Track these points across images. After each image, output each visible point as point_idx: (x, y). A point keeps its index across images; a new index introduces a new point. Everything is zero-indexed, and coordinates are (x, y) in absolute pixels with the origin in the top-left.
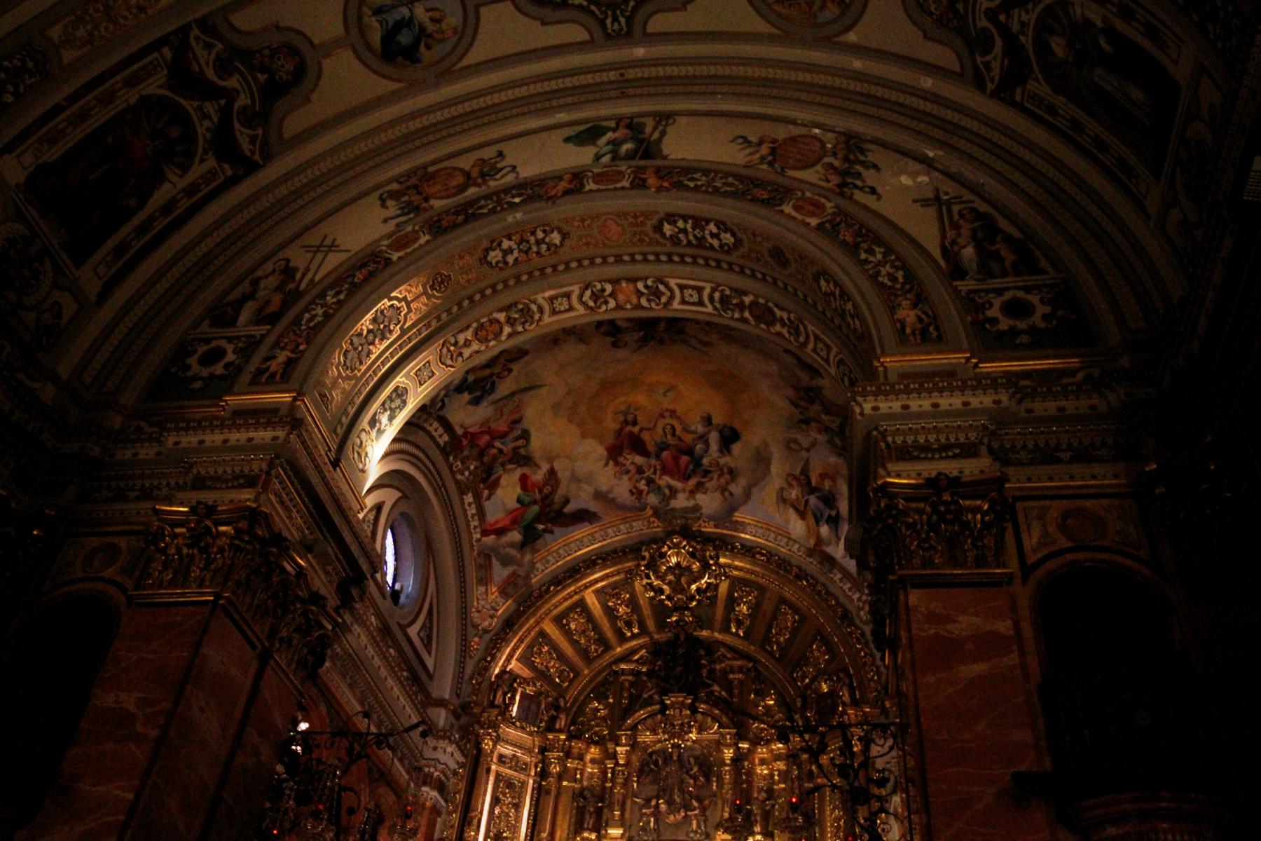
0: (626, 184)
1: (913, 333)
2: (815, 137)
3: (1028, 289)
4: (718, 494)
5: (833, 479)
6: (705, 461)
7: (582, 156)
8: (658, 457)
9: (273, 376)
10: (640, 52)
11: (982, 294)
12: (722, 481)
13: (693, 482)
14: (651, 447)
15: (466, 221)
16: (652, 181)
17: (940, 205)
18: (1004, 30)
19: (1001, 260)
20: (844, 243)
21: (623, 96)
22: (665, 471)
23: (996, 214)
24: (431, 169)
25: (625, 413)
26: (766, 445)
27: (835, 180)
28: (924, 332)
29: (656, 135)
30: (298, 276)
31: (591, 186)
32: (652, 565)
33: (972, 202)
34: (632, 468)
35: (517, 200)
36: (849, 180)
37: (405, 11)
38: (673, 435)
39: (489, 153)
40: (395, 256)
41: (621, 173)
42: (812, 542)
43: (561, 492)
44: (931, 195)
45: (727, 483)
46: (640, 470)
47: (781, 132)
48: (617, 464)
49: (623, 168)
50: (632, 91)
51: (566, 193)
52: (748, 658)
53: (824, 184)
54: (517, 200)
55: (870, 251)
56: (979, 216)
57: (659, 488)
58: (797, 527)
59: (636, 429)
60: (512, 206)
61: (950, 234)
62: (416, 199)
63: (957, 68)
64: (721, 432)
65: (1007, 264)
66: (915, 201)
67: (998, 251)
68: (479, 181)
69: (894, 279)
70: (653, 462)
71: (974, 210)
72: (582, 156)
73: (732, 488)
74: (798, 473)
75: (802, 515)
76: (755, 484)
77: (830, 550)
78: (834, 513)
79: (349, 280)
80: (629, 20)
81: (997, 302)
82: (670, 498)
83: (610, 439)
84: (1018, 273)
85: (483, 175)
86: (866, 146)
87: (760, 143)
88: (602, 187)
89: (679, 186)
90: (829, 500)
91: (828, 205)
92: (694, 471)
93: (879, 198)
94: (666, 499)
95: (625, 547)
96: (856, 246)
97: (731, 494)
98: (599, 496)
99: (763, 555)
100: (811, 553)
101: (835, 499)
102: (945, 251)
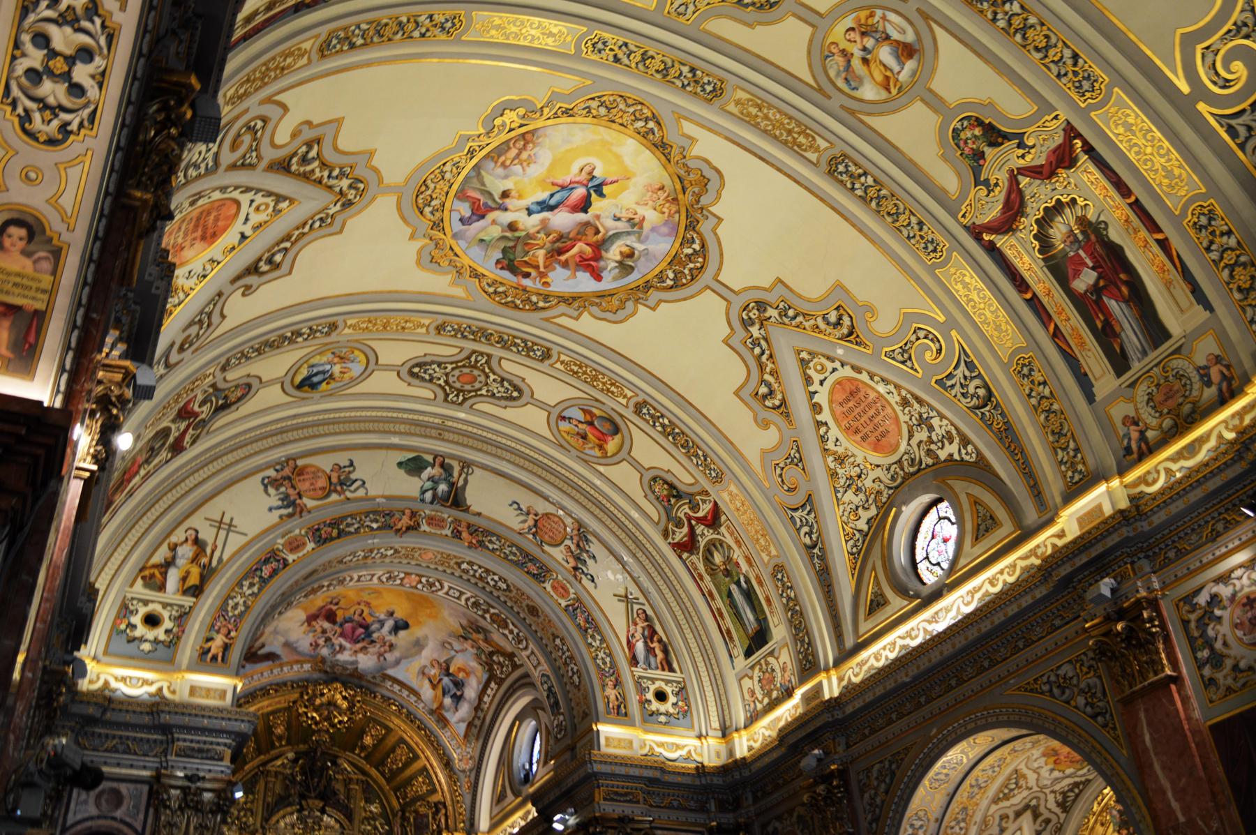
0: (448, 532)
2: (559, 517)
3: (667, 682)
4: (375, 657)
5: (468, 674)
6: (375, 635)
7: (410, 486)
8: (341, 625)
9: (214, 658)
10: (462, 415)
12: (382, 649)
13: (359, 645)
14: (339, 619)
15: (339, 536)
16: (465, 535)
17: (628, 602)
18: (692, 528)
19: (656, 656)
20: (579, 626)
21: (440, 438)
22: (342, 635)
23: (656, 621)
24: (300, 463)
25: (333, 598)
26: (426, 637)
27: (572, 563)
28: (619, 707)
29: (461, 483)
30: (209, 551)
31: (424, 527)
32: (311, 700)
33: (644, 604)
34: (319, 630)
35: (375, 526)
36: (580, 566)
37: (328, 367)
38: (361, 615)
39: (342, 458)
40: (291, 558)
41: (443, 520)
42: (435, 706)
43: (262, 640)
44: (623, 593)
45: (385, 652)
46: (324, 632)
47: (542, 507)
48: (309, 625)
49: (446, 516)
50: (447, 435)
51: (409, 528)
52: (364, 773)
53: (565, 564)
54: (375, 526)
55: (593, 637)
56: (647, 618)
57: (333, 645)
58: (427, 692)
59: (334, 608)
60: (372, 529)
61: (632, 628)
62: (291, 491)
63: (656, 519)
64: (396, 622)
65: (658, 661)
66: (615, 595)
67: (654, 649)
68: (339, 488)
69: (605, 663)
70: (337, 628)
71: (644, 611)
72: (410, 486)
73: (387, 656)
74: (441, 661)
75: (434, 687)
76: (406, 657)
77: (447, 715)
78: (459, 693)
79: (258, 573)
80: (465, 400)
81: (652, 688)
82: (338, 652)
83: (313, 610)
84: (663, 669)
85: (342, 484)
86: (590, 537)
87: (528, 513)
88: (433, 531)
89: (481, 543)
90: (459, 685)
91: (572, 591)
92: (363, 639)
93: (596, 587)
94: (334, 653)
95: (293, 682)
96: (586, 630)
97: (385, 659)
98: (287, 645)
100: (432, 712)
101: (463, 685)
102: (629, 642)
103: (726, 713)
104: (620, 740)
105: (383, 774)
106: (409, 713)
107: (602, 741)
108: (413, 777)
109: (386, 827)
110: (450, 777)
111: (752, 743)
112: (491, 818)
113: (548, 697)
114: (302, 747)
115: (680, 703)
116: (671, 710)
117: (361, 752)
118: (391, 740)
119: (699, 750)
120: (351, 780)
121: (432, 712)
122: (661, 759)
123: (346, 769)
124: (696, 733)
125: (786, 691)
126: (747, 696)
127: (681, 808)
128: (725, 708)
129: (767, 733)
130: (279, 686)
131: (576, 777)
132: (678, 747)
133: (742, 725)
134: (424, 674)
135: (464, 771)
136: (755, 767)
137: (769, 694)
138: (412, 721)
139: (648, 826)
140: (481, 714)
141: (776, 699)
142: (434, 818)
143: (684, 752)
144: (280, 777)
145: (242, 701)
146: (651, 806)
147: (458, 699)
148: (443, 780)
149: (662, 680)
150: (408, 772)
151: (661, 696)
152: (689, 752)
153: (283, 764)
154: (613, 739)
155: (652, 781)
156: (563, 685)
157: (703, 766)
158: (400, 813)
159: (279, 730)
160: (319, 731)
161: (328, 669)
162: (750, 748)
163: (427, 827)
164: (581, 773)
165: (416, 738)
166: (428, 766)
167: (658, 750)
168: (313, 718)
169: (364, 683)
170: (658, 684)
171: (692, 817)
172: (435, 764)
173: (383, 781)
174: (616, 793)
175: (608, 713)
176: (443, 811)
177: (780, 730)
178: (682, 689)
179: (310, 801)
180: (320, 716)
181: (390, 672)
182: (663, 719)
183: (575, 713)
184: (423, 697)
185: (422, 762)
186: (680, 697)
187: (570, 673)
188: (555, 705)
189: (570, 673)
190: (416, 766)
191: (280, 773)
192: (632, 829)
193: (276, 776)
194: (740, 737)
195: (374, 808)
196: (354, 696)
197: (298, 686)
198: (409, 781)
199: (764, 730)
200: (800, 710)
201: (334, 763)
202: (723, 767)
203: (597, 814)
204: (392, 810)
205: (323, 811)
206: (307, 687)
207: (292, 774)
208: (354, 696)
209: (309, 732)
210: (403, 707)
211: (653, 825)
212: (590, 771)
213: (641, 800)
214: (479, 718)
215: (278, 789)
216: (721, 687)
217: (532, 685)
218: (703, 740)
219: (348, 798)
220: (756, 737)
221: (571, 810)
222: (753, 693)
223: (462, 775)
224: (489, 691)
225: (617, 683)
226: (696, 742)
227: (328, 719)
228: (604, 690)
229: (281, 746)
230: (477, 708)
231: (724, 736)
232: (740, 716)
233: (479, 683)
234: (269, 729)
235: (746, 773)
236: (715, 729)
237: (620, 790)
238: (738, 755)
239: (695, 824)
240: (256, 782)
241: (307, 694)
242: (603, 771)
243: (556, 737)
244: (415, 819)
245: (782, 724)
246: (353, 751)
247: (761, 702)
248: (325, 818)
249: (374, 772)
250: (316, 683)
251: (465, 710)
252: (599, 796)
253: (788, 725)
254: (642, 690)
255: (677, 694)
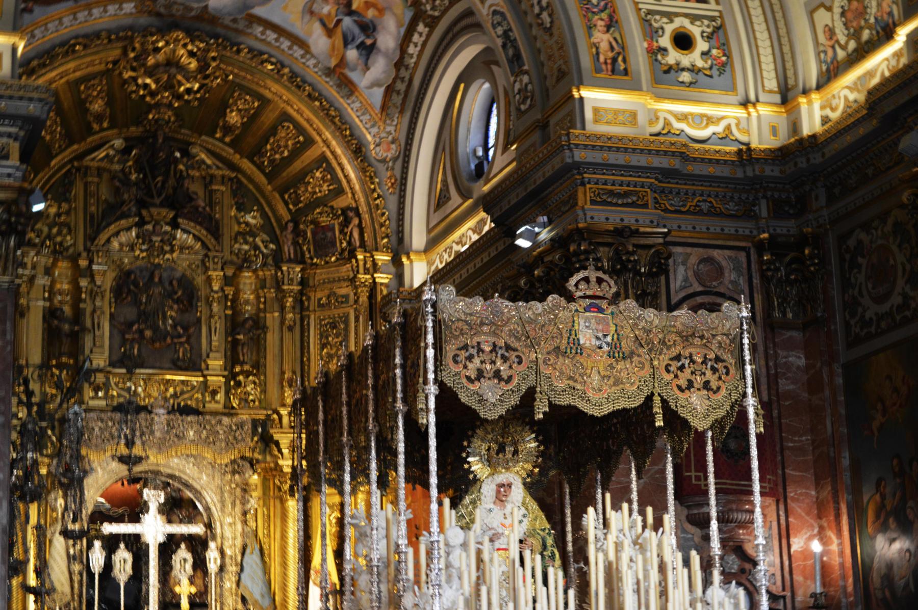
1: (606, 63)
3: (694, 18)
5: (381, 11)
11: (658, 17)
28: (614, 60)
32: (141, 58)
42: (333, 63)
52: (232, 167)
58: (319, 41)
75: (330, 32)
77: (354, 76)
78: (369, 42)
81: (669, 29)
90: (368, 28)
95: (109, 32)
99: (272, 64)
100: (329, 72)
101: (375, 29)
103: (789, 65)
104: (616, 112)
105: (260, 167)
106: (294, 75)
107: (589, 114)
108: (306, 172)
109: (272, 246)
110: (364, 171)
111: (828, 112)
112: (429, 231)
113: (504, 46)
114: (134, 130)
115: (714, 52)
116: (700, 63)
117: (224, 136)
118: (268, 118)
119: (744, 124)
120: (212, 177)
121: (329, 72)
122: (683, 139)
123: (203, 162)
124: (740, 97)
125: (884, 29)
126: (822, 38)
127: (713, 213)
128: (788, 57)
129: (852, 96)
130: (90, 39)
131: (548, 170)
132: (710, 120)
133: (813, 83)
134: (312, 13)
135: (383, 161)
136: (830, 151)
137: (855, 35)
138: (299, 87)
139: (661, 240)
140: (404, 73)
141: (867, 42)
142: (341, 232)
143: (719, 128)
144: (106, 176)
145: (35, 63)
146: (666, 210)
147: (368, 50)
148: (352, 175)
149: (686, 15)
150: (298, 165)
151: (683, 41)
152: (728, 127)
153: (107, 156)
154: (606, 110)
155: (667, 174)
156: (526, 28)
157: (749, 149)
158: (291, 225)
159: (97, 106)
160: (158, 105)
161: (162, 10)
162: (825, 120)
163: (333, 244)
164: (556, 163)
165: (308, 113)
166: (329, 154)
167: (678, 125)
168: (146, 86)
169: (219, 30)
170: (679, 22)
171: (730, 227)
172: (339, 151)
173: (261, 179)
174: (611, 193)
175: (598, 70)
176: (356, 221)
177: (870, 93)
178: (717, 29)
179: (154, 211)
180: (157, 82)
181: (259, 11)
182: (686, 77)
183: (546, 71)
184: (314, 49)
185: (320, 148)
186: (714, 42)
187: (537, 10)
188: (516, 60)
189: (537, 10)
190: (311, 154)
191: (104, 169)
192: (634, 245)
193: (99, 175)
194: (810, 103)
195: (252, 219)
196: (206, 51)
197: (118, 39)
198: (301, 177)
199: (846, 92)
200: (904, 61)
201: (185, 153)
202: (781, 149)
203: (581, 225)
204: (279, 219)
205: (175, 225)
206: (132, 39)
207: (123, 170)
208: (206, 51)
209: (139, 109)
210: (283, 66)
211: (669, 239)
212: (569, 160)
213: (651, 203)
214: (402, 79)
215: (105, 193)
216: (781, 24)
217: (478, 26)
218: (751, 109)
219: (211, 204)
220: (834, 103)
221: (543, 219)
222: (831, 32)
223: (381, 167)
224: (416, 38)
225: (612, 24)
226: (740, 113)
227: (170, 86)
228: (590, 36)
229: (102, 130)
230: (399, 64)
231: (784, 101)
232: (811, 71)
233: (399, 25)
234: (81, 105)
235: (817, 159)
236: (771, 92)
237: (617, 188)
238: (806, 131)
239: (736, 237)
240: (71, 183)
241: (134, 49)
242: (590, 159)
243: (518, 109)
244: (314, 233)
245: (876, 81)
246: (212, 134)
247: (844, 48)
248: (179, 234)
249: (246, 165)
250: (146, 32)
251: (379, 68)
252: (583, 197)
253: (885, 82)
254: (652, 33)
255: (709, 38)
